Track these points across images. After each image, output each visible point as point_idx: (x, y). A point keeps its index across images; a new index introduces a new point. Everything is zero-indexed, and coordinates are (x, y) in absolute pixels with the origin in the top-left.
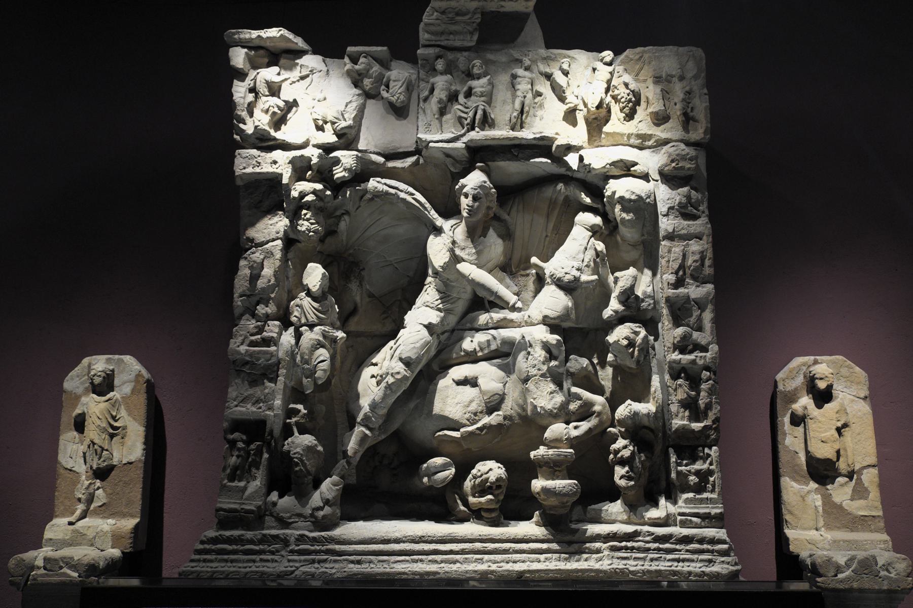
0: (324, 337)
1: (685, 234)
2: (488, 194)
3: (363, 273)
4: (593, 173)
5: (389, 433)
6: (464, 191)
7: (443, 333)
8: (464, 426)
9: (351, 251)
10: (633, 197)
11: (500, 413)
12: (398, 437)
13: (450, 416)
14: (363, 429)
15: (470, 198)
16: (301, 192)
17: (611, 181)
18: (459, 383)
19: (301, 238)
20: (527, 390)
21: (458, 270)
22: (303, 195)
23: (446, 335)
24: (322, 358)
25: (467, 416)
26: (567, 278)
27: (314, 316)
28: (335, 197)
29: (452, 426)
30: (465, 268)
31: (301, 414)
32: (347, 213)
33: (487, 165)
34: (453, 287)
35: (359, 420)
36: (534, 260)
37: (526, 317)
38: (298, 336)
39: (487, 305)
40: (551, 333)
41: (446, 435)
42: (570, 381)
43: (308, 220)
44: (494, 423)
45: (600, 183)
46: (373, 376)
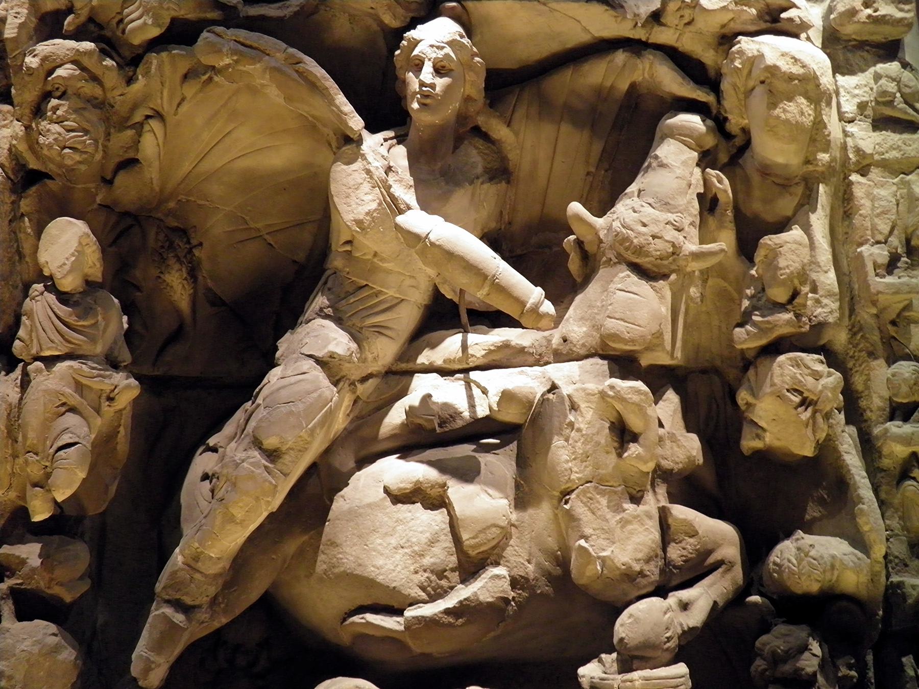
0: (80, 388)
1: (897, 161)
2: (470, 66)
3: (196, 252)
4: (701, 23)
5: (238, 612)
6: (415, 52)
7: (364, 380)
8: (414, 602)
9: (172, 205)
10: (796, 70)
11: (501, 571)
12: (271, 610)
13: (380, 579)
14: (168, 611)
15: (428, 68)
16: (44, 59)
17: (740, 38)
18: (399, 498)
19: (51, 168)
20: (571, 517)
21: (398, 227)
22: (50, 66)
23: (371, 382)
24: (66, 439)
25: (422, 577)
26: (658, 247)
27: (57, 338)
28: (130, 81)
29: (384, 601)
30: (417, 220)
31: (25, 570)
32: (158, 115)
33: (463, 7)
34: (388, 272)
35: (159, 587)
36: (576, 207)
37: (556, 341)
38: (25, 383)
39: (464, 318)
40: (623, 378)
41: (369, 624)
42: (662, 490)
43: (59, 122)
44: (486, 597)
45: (708, 57)
46: (205, 477)
